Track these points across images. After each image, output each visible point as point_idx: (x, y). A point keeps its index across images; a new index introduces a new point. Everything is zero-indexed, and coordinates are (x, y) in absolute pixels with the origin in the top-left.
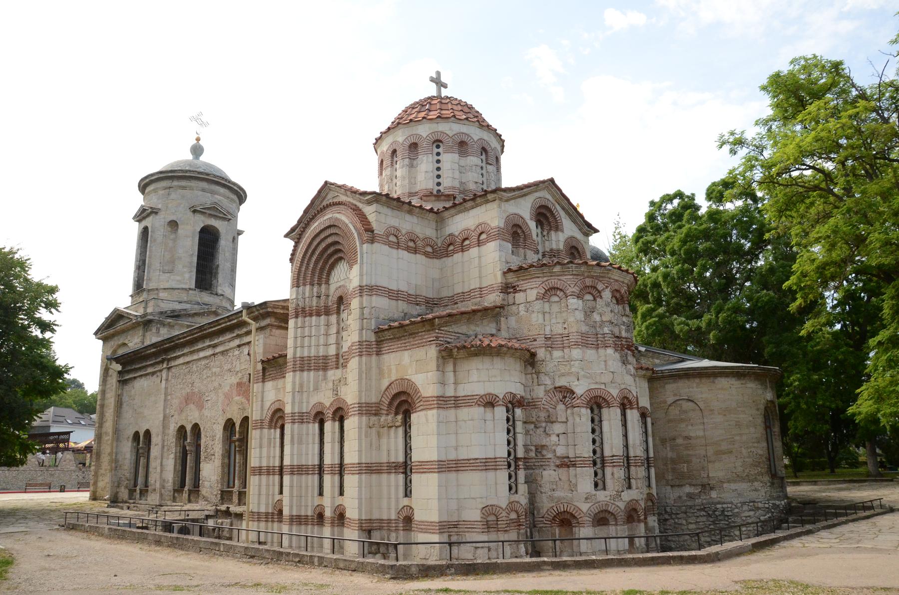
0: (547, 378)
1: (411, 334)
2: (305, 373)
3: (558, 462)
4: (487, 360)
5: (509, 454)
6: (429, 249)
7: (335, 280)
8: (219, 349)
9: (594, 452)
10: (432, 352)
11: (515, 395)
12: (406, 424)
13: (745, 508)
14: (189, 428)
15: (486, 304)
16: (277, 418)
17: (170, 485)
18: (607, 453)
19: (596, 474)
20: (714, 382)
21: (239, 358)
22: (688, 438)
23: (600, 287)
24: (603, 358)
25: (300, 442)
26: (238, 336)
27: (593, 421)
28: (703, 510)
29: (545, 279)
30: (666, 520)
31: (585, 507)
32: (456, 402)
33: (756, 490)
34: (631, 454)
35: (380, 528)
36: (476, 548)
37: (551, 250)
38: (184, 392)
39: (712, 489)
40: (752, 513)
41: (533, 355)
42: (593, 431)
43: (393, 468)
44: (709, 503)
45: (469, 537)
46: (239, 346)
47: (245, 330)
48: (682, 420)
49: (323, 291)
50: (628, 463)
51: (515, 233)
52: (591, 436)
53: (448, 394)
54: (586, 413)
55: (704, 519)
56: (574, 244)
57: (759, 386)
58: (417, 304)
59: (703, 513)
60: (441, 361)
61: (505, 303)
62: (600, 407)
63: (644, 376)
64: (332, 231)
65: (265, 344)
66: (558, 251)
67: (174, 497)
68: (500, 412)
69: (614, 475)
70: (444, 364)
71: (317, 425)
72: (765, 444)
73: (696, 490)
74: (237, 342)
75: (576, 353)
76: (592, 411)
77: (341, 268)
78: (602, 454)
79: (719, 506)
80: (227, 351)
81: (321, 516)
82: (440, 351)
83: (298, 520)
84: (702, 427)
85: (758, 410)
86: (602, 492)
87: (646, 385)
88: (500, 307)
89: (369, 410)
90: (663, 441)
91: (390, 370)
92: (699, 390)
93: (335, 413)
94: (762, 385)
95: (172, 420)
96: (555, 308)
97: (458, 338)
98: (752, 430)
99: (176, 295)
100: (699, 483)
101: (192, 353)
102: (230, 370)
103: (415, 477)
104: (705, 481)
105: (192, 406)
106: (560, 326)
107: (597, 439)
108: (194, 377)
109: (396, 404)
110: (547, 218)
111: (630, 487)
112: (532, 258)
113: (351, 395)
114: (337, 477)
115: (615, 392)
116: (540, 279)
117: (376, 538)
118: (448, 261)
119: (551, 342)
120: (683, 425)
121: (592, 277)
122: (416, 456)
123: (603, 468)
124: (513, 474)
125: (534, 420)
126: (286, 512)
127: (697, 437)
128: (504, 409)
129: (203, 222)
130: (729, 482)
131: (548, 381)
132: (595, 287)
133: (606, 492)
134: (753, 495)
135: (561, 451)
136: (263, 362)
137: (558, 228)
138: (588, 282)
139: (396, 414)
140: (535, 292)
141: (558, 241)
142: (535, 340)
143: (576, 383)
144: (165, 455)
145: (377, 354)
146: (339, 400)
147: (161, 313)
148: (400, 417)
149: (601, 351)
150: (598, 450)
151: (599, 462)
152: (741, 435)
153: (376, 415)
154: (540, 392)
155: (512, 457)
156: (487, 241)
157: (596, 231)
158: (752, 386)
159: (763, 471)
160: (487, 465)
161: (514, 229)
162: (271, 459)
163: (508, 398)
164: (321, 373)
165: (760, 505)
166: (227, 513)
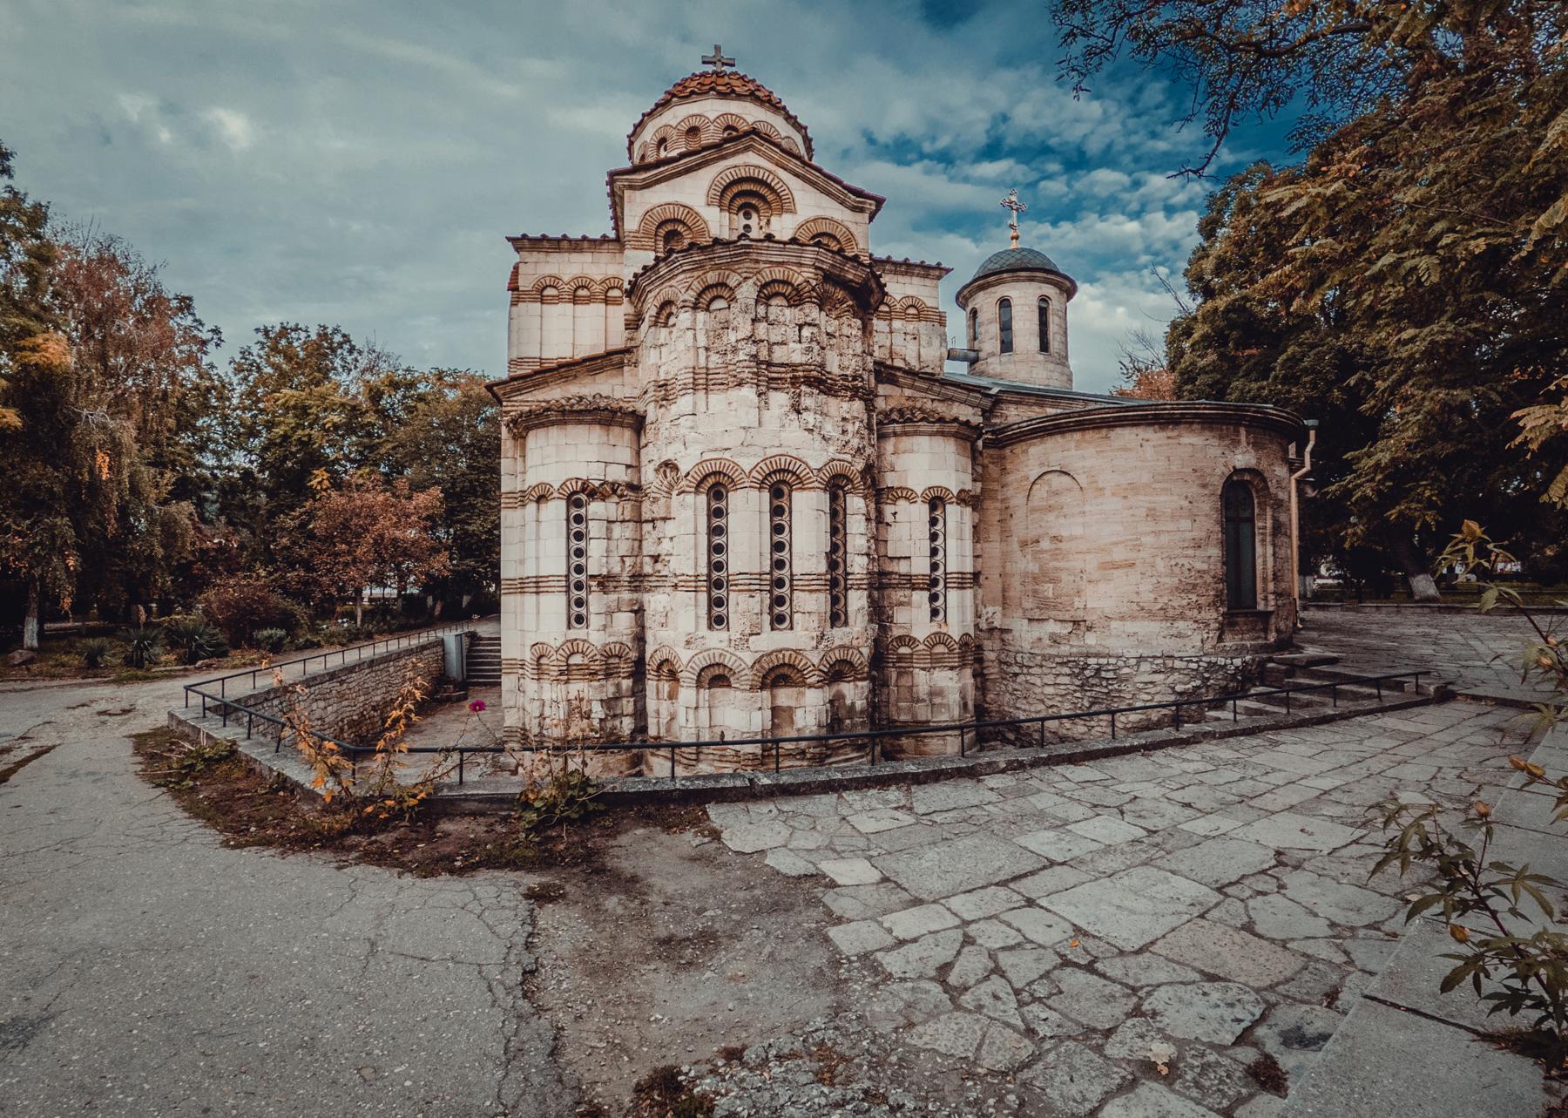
4: (541, 432)
13: (1145, 667)
20: (1107, 437)
22: (1056, 539)
23: (732, 282)
30: (1016, 675)
31: (684, 656)
33: (1179, 636)
39: (1089, 629)
40: (1159, 678)
41: (644, 418)
44: (1081, 655)
48: (1050, 508)
55: (1066, 680)
57: (1215, 442)
59: (1066, 670)
63: (942, 434)
68: (555, 510)
72: (1215, 552)
73: (1064, 630)
79: (1092, 661)
85: (1204, 486)
90: (1024, 544)
94: (1221, 438)
98: (1186, 524)
100: (1067, 617)
104: (1080, 615)
110: (763, 198)
115: (747, 464)
120: (1051, 517)
121: (718, 267)
127: (1072, 538)
128: (563, 503)
130: (1122, 618)
134: (1170, 646)
138: (712, 277)
151: (715, 585)
152: (1156, 533)
157: (879, 202)
159: (1202, 601)
163: (570, 487)
165: (1178, 664)
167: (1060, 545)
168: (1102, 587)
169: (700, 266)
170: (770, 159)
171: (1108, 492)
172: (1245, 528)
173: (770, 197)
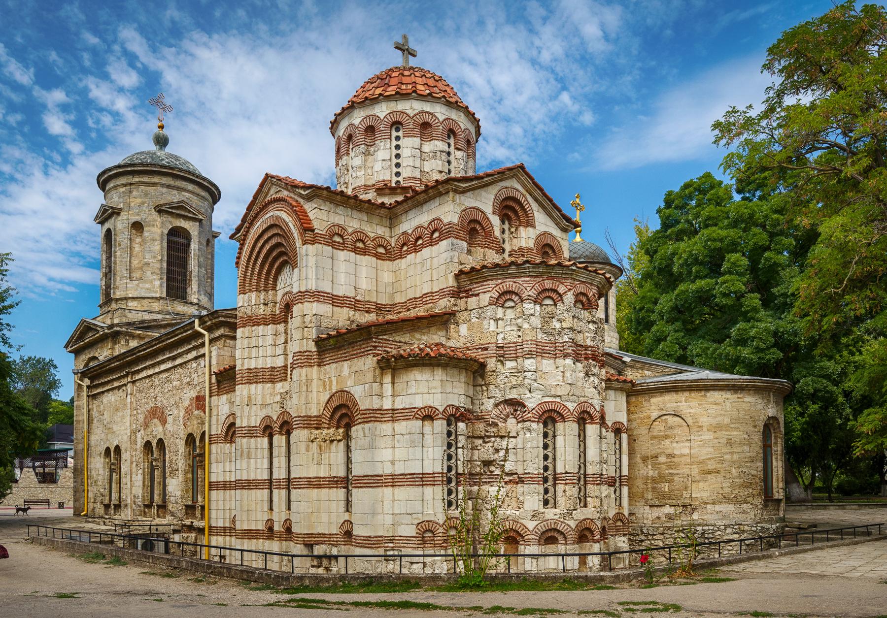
0: (497, 391)
1: (350, 344)
2: (253, 386)
3: (507, 479)
5: (450, 469)
6: (381, 250)
7: (282, 285)
8: (179, 361)
9: (546, 468)
10: (369, 362)
11: (458, 408)
12: (347, 437)
14: (154, 443)
15: (437, 311)
16: (231, 432)
17: (139, 500)
18: (560, 469)
19: (546, 491)
21: (196, 371)
24: (561, 369)
25: (249, 458)
26: (195, 348)
27: (546, 435)
28: (682, 531)
29: (500, 281)
31: (531, 525)
32: (394, 415)
34: (590, 470)
35: (323, 543)
36: (412, 563)
37: (520, 249)
38: (148, 407)
39: (694, 510)
41: (483, 366)
42: (546, 447)
43: (335, 482)
44: (690, 525)
45: (405, 551)
46: (196, 358)
47: (201, 341)
49: (270, 297)
50: (585, 481)
51: (473, 229)
52: (542, 452)
53: (385, 407)
54: (538, 427)
56: (549, 241)
58: (367, 312)
60: (378, 371)
61: (455, 308)
62: (554, 421)
64: (275, 231)
65: (218, 355)
66: (529, 250)
67: (144, 512)
68: (440, 425)
69: (565, 494)
70: (382, 374)
71: (266, 440)
74: (194, 354)
75: (529, 363)
76: (545, 425)
77: (287, 270)
78: (555, 471)
80: (185, 363)
81: (271, 529)
82: (379, 362)
83: (249, 534)
84: (688, 444)
86: (554, 511)
87: (624, 398)
88: (450, 314)
89: (312, 423)
91: (331, 382)
92: (687, 404)
93: (281, 427)
95: (139, 435)
96: (510, 314)
97: (400, 347)
99: (145, 305)
101: (153, 366)
102: (188, 383)
103: (354, 491)
104: (688, 501)
105: (156, 421)
106: (515, 334)
107: (550, 454)
108: (157, 391)
109: (337, 416)
111: (585, 506)
112: (493, 257)
113: (295, 407)
114: (284, 492)
115: (571, 406)
116: (494, 282)
117: (319, 550)
118: (403, 263)
119: (503, 353)
122: (357, 470)
123: (555, 485)
124: (454, 490)
125: (483, 434)
126: (238, 527)
129: (171, 223)
131: (498, 395)
132: (555, 291)
133: (557, 511)
135: (508, 467)
136: (216, 374)
137: (530, 223)
139: (337, 428)
140: (488, 295)
141: (526, 238)
142: (486, 349)
143: (529, 395)
144: (134, 470)
145: (319, 366)
146: (285, 412)
147: (129, 324)
148: (341, 430)
149: (560, 361)
150: (551, 466)
151: (549, 478)
153: (317, 428)
154: (489, 404)
155: (453, 472)
156: (440, 239)
158: (749, 400)
160: (422, 480)
161: (472, 226)
162: (228, 474)
163: (450, 411)
164: (269, 385)
166: (191, 528)
167: (675, 460)
168: (701, 485)
169: (541, 275)
170: (524, 186)
171: (705, 429)
172: (769, 449)
173: (521, 213)
